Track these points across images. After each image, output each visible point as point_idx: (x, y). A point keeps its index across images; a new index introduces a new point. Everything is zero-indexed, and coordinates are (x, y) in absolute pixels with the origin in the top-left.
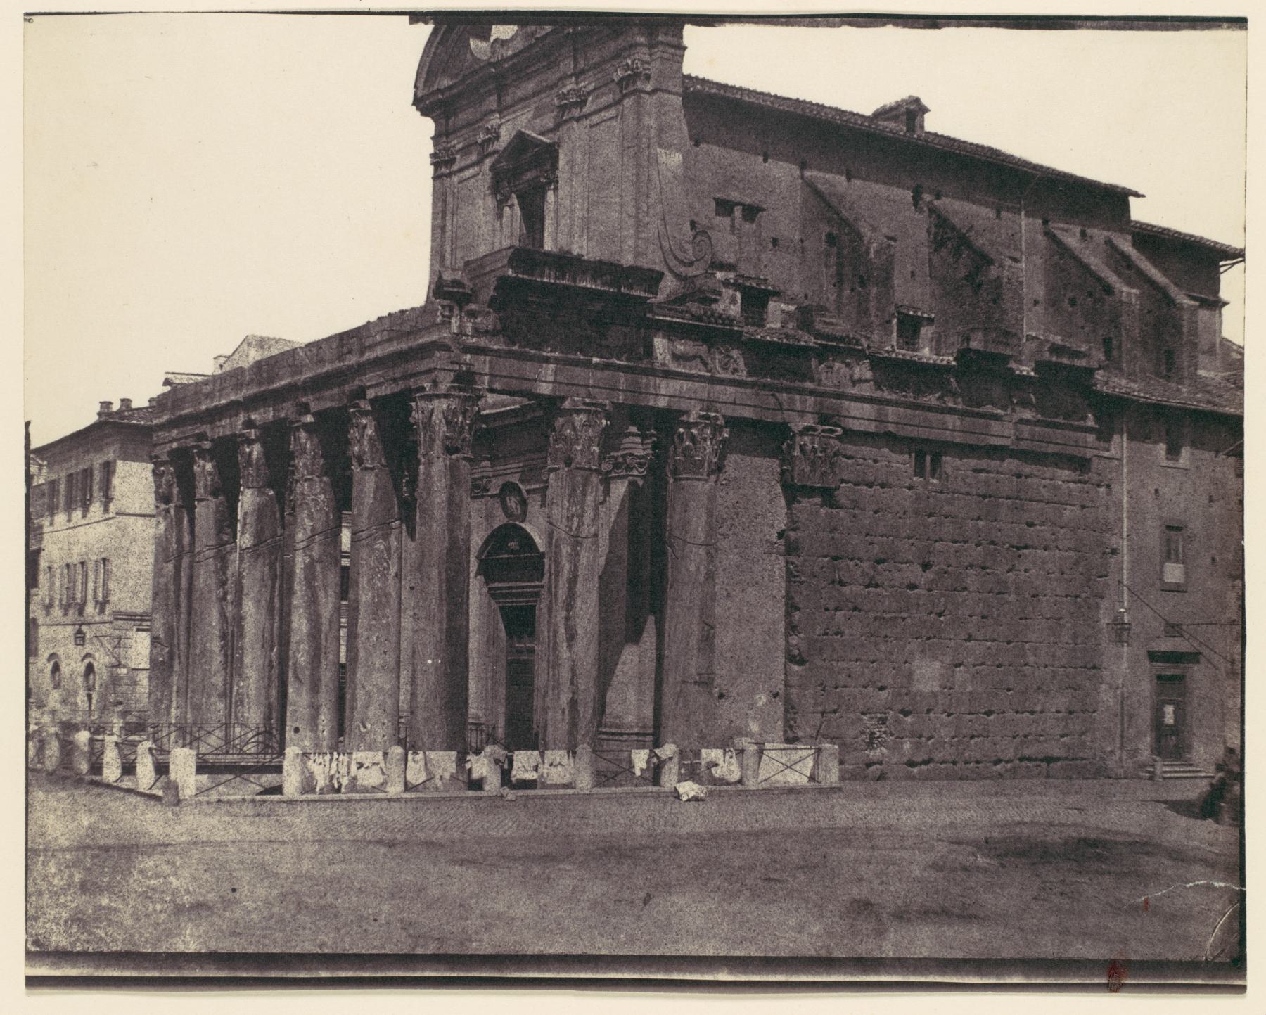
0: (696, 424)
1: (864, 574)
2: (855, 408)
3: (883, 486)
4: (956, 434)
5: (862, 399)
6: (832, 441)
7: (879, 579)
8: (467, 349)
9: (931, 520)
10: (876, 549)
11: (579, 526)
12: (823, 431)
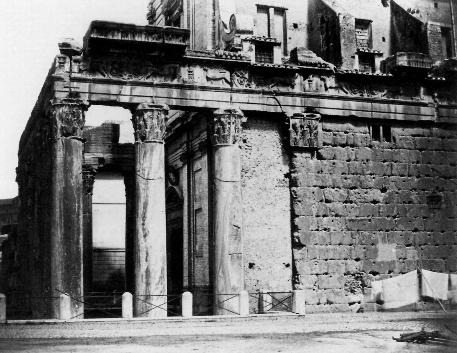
1: (341, 196)
2: (326, 103)
3: (352, 146)
4: (398, 115)
5: (331, 98)
6: (313, 121)
7: (352, 198)
8: (73, 80)
9: (386, 164)
10: (349, 181)
12: (307, 116)
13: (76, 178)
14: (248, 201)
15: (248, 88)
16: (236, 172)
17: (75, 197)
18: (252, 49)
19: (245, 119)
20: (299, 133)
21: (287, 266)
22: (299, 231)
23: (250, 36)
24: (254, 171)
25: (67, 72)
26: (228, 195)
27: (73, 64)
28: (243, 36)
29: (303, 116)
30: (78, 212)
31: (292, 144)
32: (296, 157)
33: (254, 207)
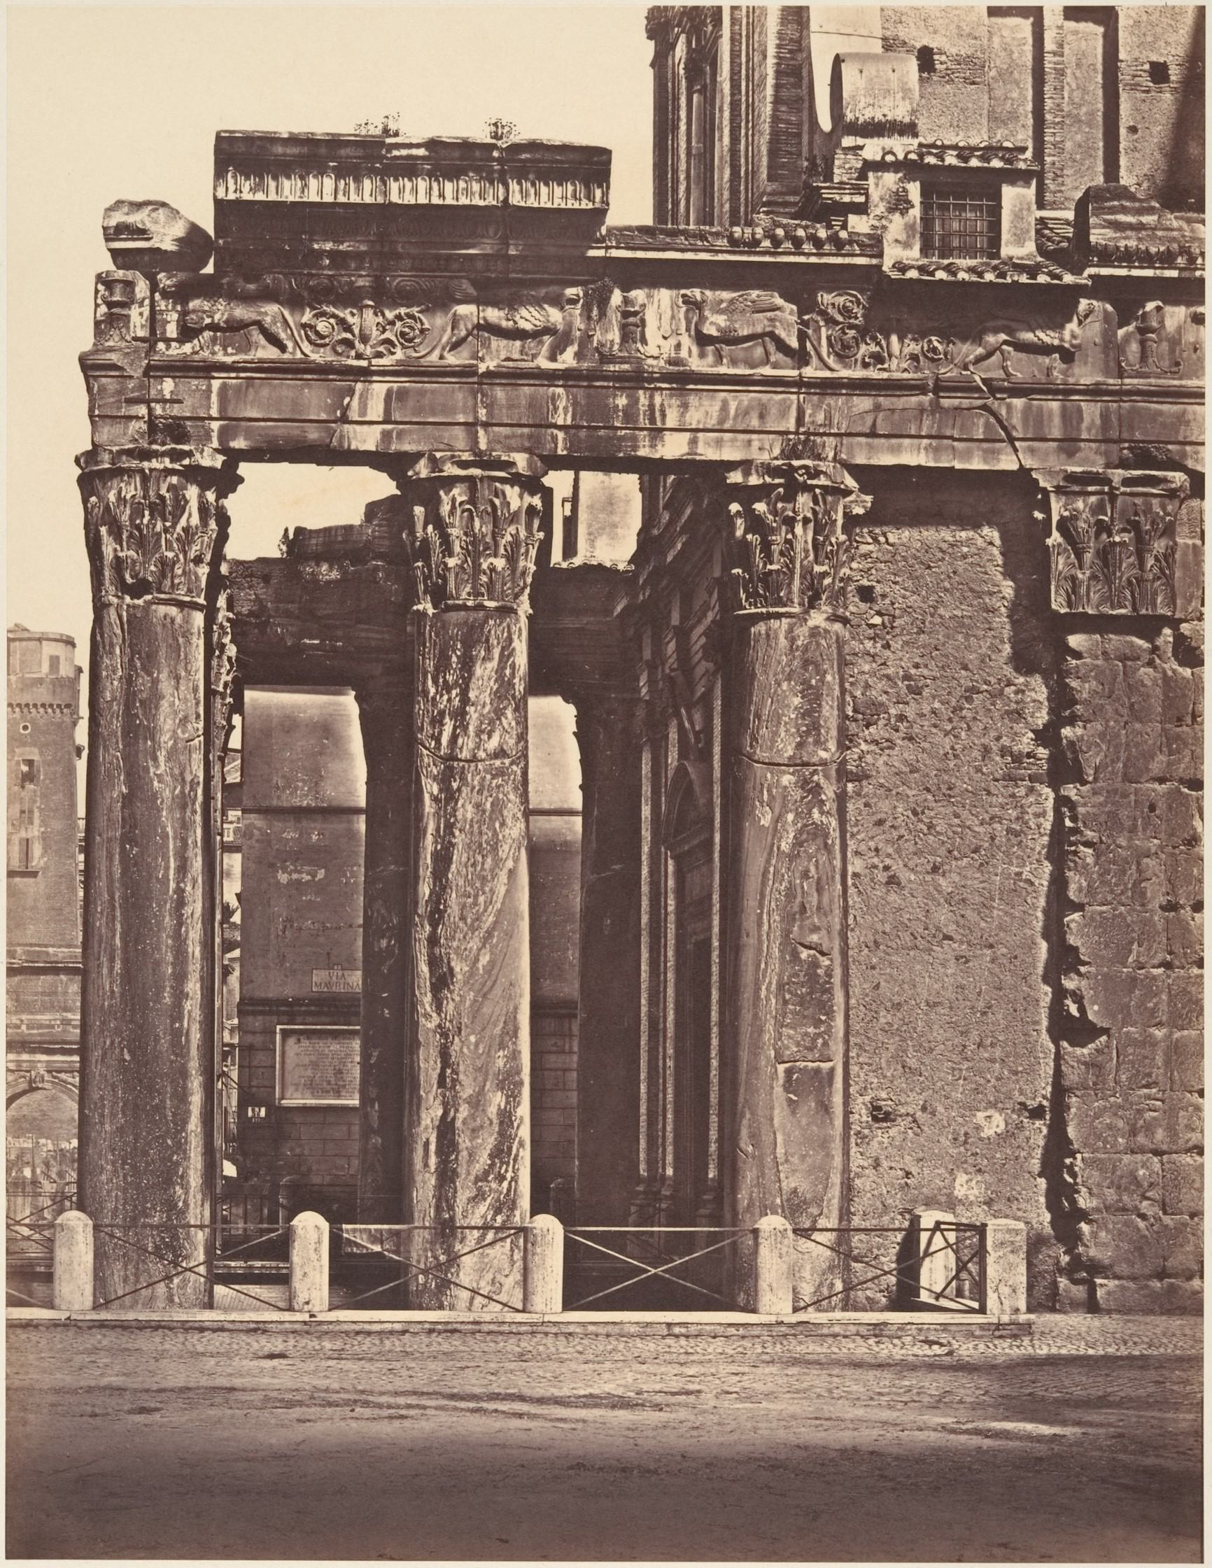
0: (763, 492)
6: (1155, 501)
11: (454, 739)
12: (1127, 482)
13: (168, 759)
14: (872, 844)
15: (873, 374)
16: (815, 727)
17: (165, 836)
18: (908, 202)
19: (861, 504)
20: (1088, 557)
21: (1037, 1113)
22: (1083, 969)
23: (900, 146)
24: (901, 718)
25: (136, 339)
26: (777, 820)
27: (162, 305)
28: (873, 149)
29: (1108, 482)
30: (180, 891)
31: (1058, 604)
32: (1078, 655)
33: (897, 866)
